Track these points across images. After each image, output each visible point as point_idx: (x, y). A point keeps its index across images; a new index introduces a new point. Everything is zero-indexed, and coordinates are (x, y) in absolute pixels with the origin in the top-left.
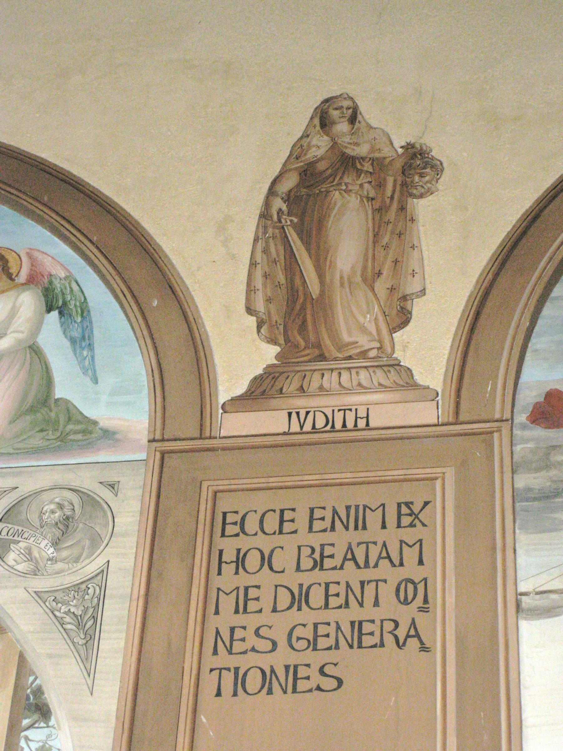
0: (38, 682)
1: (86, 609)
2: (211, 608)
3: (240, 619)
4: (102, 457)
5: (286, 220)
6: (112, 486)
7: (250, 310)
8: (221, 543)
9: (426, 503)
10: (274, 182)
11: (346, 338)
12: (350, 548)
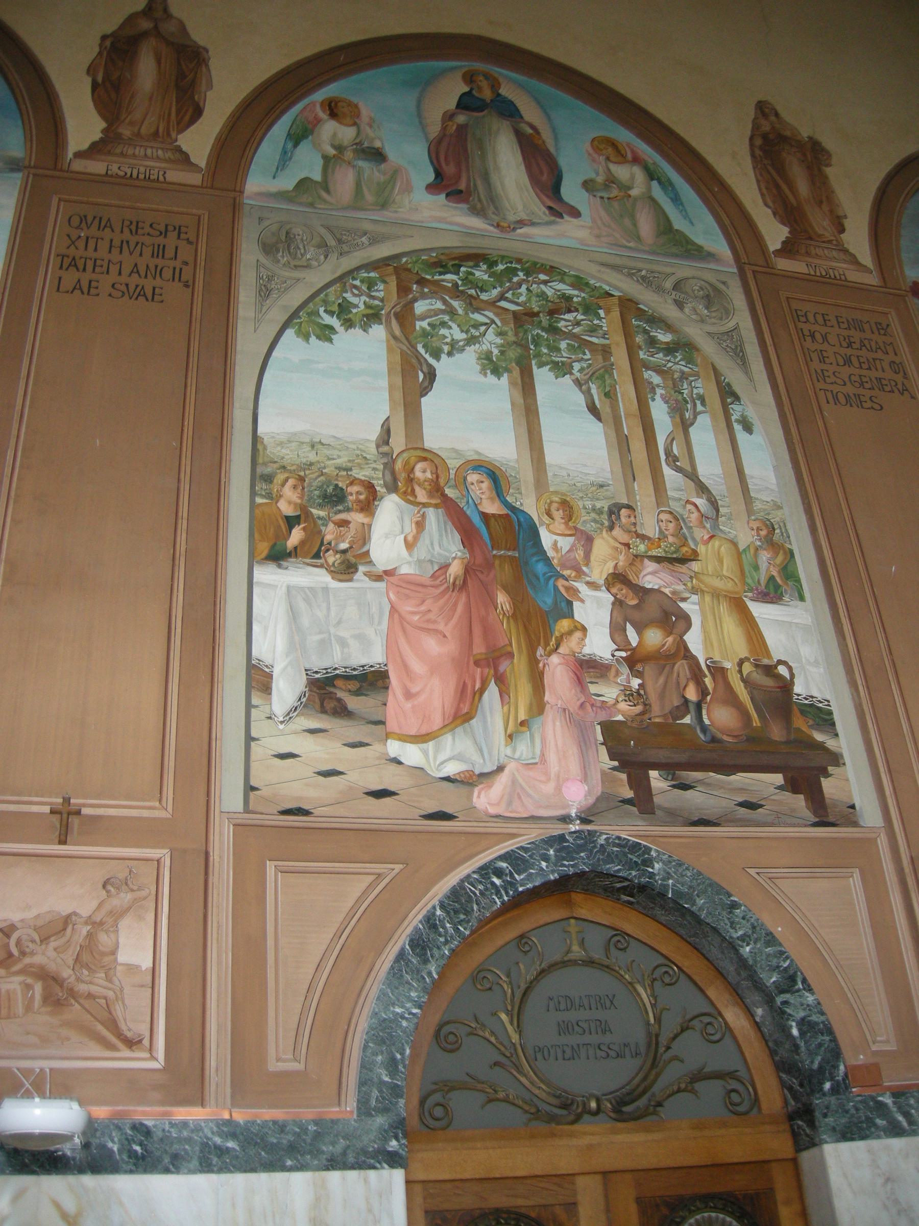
0: (726, 380)
1: (736, 347)
2: (809, 359)
3: (825, 367)
4: (712, 266)
5: (766, 162)
6: (724, 283)
7: (766, 205)
8: (801, 325)
9: (888, 325)
10: (751, 139)
11: (820, 232)
12: (861, 341)
